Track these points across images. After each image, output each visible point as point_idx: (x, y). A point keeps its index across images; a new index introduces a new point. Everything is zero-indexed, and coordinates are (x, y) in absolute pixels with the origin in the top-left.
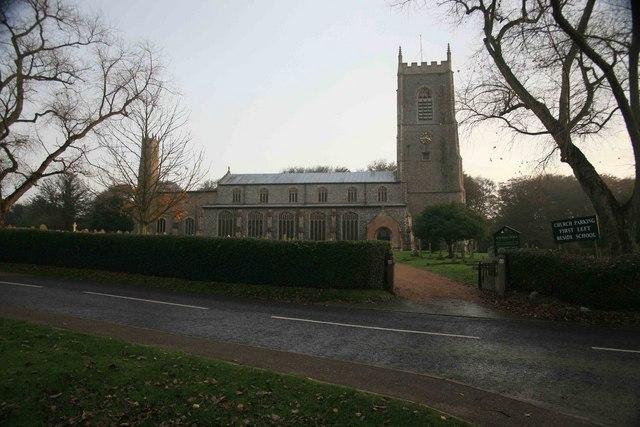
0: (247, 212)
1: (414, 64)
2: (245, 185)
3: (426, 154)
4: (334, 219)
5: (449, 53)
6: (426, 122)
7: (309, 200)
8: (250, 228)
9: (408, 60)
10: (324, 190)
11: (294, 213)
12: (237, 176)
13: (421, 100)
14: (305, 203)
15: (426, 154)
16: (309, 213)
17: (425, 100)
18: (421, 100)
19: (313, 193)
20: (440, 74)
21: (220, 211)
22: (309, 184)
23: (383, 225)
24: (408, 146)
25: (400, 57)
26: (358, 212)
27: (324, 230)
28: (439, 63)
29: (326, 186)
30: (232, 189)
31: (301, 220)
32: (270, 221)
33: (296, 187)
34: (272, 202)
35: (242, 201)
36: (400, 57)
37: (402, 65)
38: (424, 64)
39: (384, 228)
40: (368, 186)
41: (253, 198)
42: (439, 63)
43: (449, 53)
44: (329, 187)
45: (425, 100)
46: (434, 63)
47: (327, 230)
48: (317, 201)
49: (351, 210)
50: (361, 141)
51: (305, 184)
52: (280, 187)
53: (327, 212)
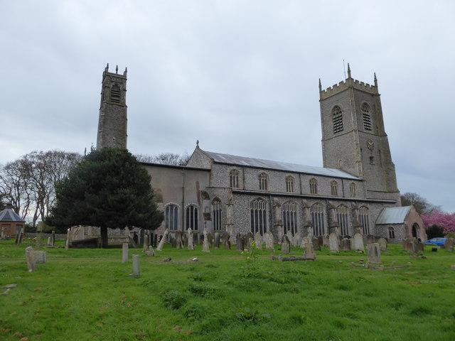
5: (376, 81)
20: (373, 95)
29: (315, 177)
33: (292, 175)
34: (271, 189)
36: (349, 71)
43: (376, 81)
48: (309, 193)
52: (281, 173)
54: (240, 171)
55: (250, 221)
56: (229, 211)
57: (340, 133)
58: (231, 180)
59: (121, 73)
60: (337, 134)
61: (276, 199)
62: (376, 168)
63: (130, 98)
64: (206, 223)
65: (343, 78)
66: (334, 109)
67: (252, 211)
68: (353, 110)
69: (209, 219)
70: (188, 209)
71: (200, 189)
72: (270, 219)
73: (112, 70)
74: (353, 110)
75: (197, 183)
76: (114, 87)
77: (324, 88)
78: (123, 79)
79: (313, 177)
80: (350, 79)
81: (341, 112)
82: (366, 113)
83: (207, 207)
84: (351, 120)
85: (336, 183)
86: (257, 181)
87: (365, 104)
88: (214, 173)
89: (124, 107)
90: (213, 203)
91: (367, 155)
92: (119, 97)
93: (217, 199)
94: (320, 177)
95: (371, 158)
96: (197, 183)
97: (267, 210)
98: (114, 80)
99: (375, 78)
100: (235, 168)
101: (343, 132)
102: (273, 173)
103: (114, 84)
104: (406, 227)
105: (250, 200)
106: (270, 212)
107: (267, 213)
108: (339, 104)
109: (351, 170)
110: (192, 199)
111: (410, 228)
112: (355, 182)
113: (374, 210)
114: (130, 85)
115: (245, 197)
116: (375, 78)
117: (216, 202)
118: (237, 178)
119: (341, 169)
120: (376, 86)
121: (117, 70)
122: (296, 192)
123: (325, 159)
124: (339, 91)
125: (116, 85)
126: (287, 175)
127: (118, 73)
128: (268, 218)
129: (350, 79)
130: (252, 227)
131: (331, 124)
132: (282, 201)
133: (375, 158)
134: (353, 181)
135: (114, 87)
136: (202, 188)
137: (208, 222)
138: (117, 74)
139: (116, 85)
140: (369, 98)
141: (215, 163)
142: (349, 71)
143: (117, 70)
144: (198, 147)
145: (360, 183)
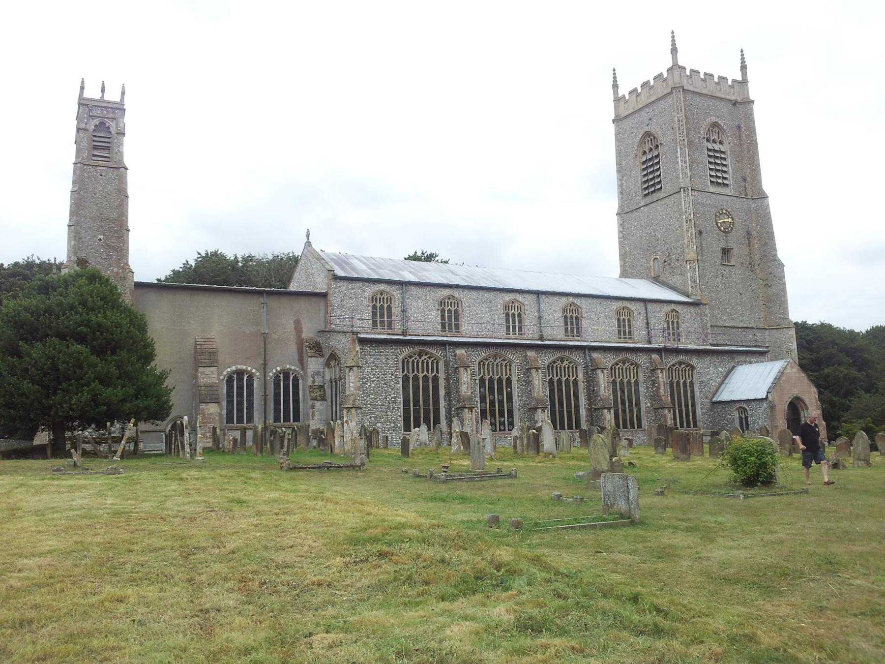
3: (726, 252)
5: (744, 67)
7: (547, 332)
8: (483, 399)
9: (687, 61)
14: (541, 338)
19: (553, 312)
20: (735, 103)
21: (406, 351)
24: (700, 233)
29: (577, 301)
33: (520, 298)
34: (469, 331)
35: (398, 327)
36: (674, 50)
43: (744, 67)
44: (583, 303)
48: (563, 337)
49: (681, 358)
51: (538, 293)
52: (492, 295)
54: (395, 292)
55: (401, 400)
56: (352, 382)
57: (655, 196)
58: (374, 315)
59: (112, 96)
60: (649, 199)
61: (460, 352)
62: (738, 274)
63: (133, 151)
64: (313, 407)
65: (663, 65)
66: (642, 141)
67: (406, 379)
69: (323, 398)
70: (277, 378)
71: (305, 335)
72: (448, 394)
73: (92, 93)
75: (298, 323)
76: (100, 133)
77: (624, 91)
78: (118, 109)
79: (571, 299)
80: (676, 67)
81: (657, 147)
82: (717, 147)
83: (318, 373)
84: (678, 166)
85: (630, 312)
86: (434, 315)
87: (715, 125)
88: (334, 300)
89: (120, 168)
90: (327, 365)
91: (715, 243)
92: (108, 148)
93: (333, 357)
94: (590, 300)
95: (726, 252)
96: (298, 323)
97: (442, 376)
98: (97, 112)
100: (383, 287)
101: (662, 195)
102: (474, 294)
103: (96, 121)
104: (772, 407)
105: (401, 357)
106: (447, 379)
107: (442, 383)
108: (654, 129)
109: (676, 280)
110: (284, 359)
111: (782, 410)
112: (678, 308)
113: (706, 371)
114: (130, 122)
115: (386, 350)
116: (743, 59)
117: (332, 363)
118: (389, 308)
119: (656, 280)
120: (744, 82)
121: (103, 91)
122: (530, 336)
123: (623, 256)
124: (654, 98)
125: (102, 124)
126: (508, 297)
127: (106, 98)
128: (442, 392)
129: (676, 67)
130: (406, 412)
131: (637, 175)
132: (608, 360)
133: (735, 252)
134: (673, 306)
135: (100, 133)
136: (308, 333)
137: (318, 404)
138: (102, 100)
139: (102, 124)
140: (726, 109)
141: (336, 278)
142: (674, 50)
143: (103, 91)
144: (308, 244)
145: (692, 309)
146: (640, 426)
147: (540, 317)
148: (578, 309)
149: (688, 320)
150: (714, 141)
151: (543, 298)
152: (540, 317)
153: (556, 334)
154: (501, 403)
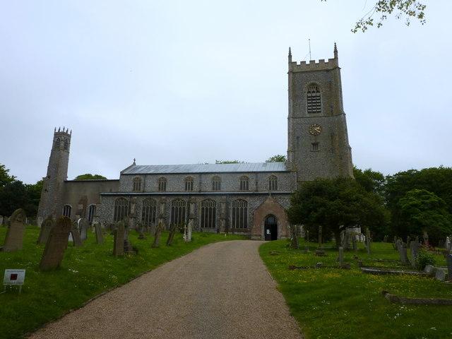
0: (142, 199)
1: (303, 63)
2: (146, 175)
4: (223, 206)
5: (336, 52)
6: (315, 114)
8: (143, 215)
9: (297, 59)
10: (216, 177)
11: (186, 199)
12: (140, 167)
13: (309, 95)
15: (315, 145)
16: (200, 199)
17: (314, 95)
18: (309, 95)
19: (207, 182)
22: (202, 173)
23: (271, 212)
24: (298, 138)
25: (290, 56)
26: (248, 199)
27: (214, 217)
28: (326, 61)
30: (133, 177)
31: (192, 207)
32: (162, 208)
33: (192, 176)
34: (169, 190)
35: (142, 190)
36: (290, 56)
37: (292, 64)
38: (312, 62)
39: (271, 215)
40: (259, 175)
41: (152, 187)
42: (326, 61)
43: (336, 52)
44: (222, 176)
45: (314, 95)
46: (322, 61)
47: (217, 217)
49: (241, 197)
50: (256, 134)
53: (218, 199)
54: (142, 178)
67: (116, 207)
68: (315, 92)
74: (315, 92)
76: (62, 142)
85: (248, 179)
86: (156, 185)
87: (313, 84)
94: (226, 175)
99: (335, 47)
102: (172, 176)
112: (276, 175)
116: (335, 47)
146: (214, 226)
147: (201, 183)
148: (220, 179)
149: (282, 180)
150: (313, 92)
151: (203, 176)
152: (201, 183)
153: (208, 189)
154: (150, 216)
